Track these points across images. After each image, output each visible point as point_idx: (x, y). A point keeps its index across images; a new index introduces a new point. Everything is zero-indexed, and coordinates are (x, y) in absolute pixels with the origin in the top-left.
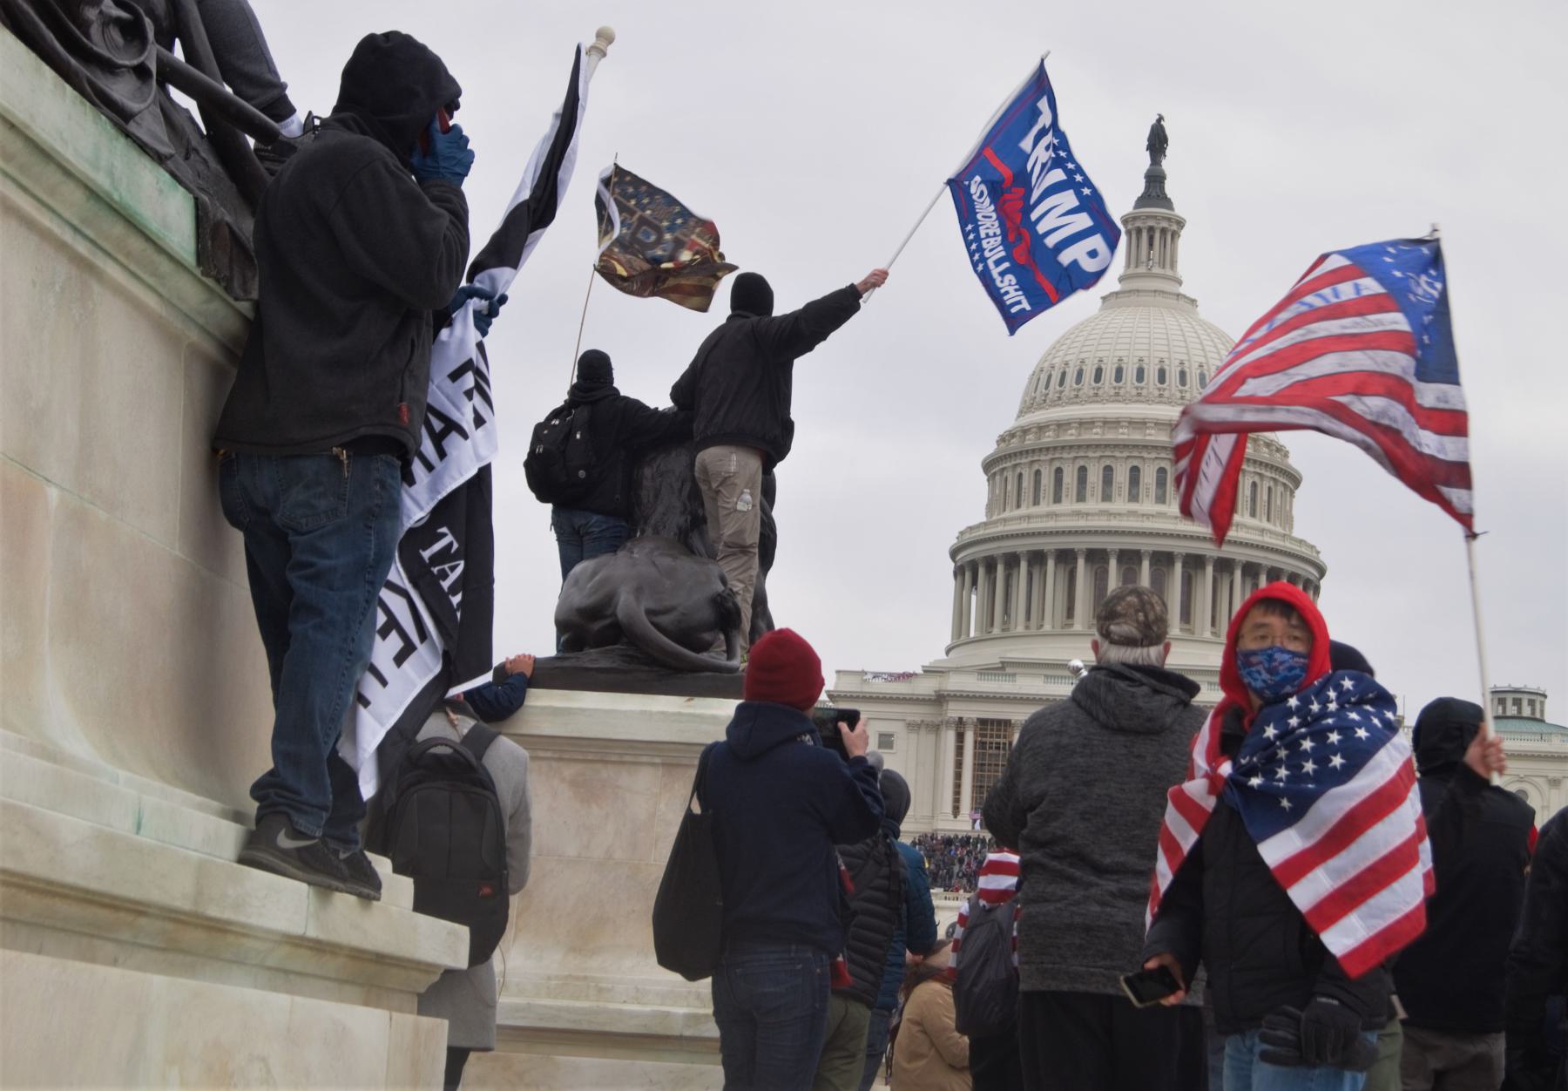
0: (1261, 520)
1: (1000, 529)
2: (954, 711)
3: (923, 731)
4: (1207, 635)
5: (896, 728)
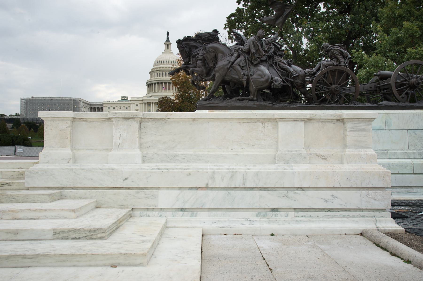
1: (151, 80)
2: (144, 101)
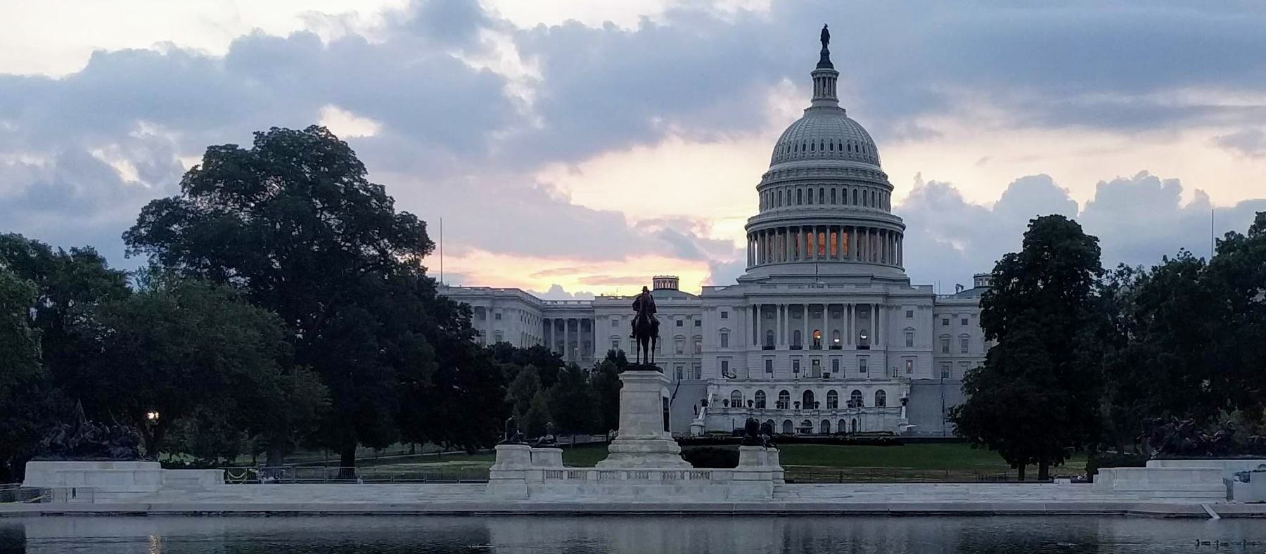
0: (877, 208)
2: (752, 301)
3: (740, 310)
4: (856, 260)
5: (728, 309)
